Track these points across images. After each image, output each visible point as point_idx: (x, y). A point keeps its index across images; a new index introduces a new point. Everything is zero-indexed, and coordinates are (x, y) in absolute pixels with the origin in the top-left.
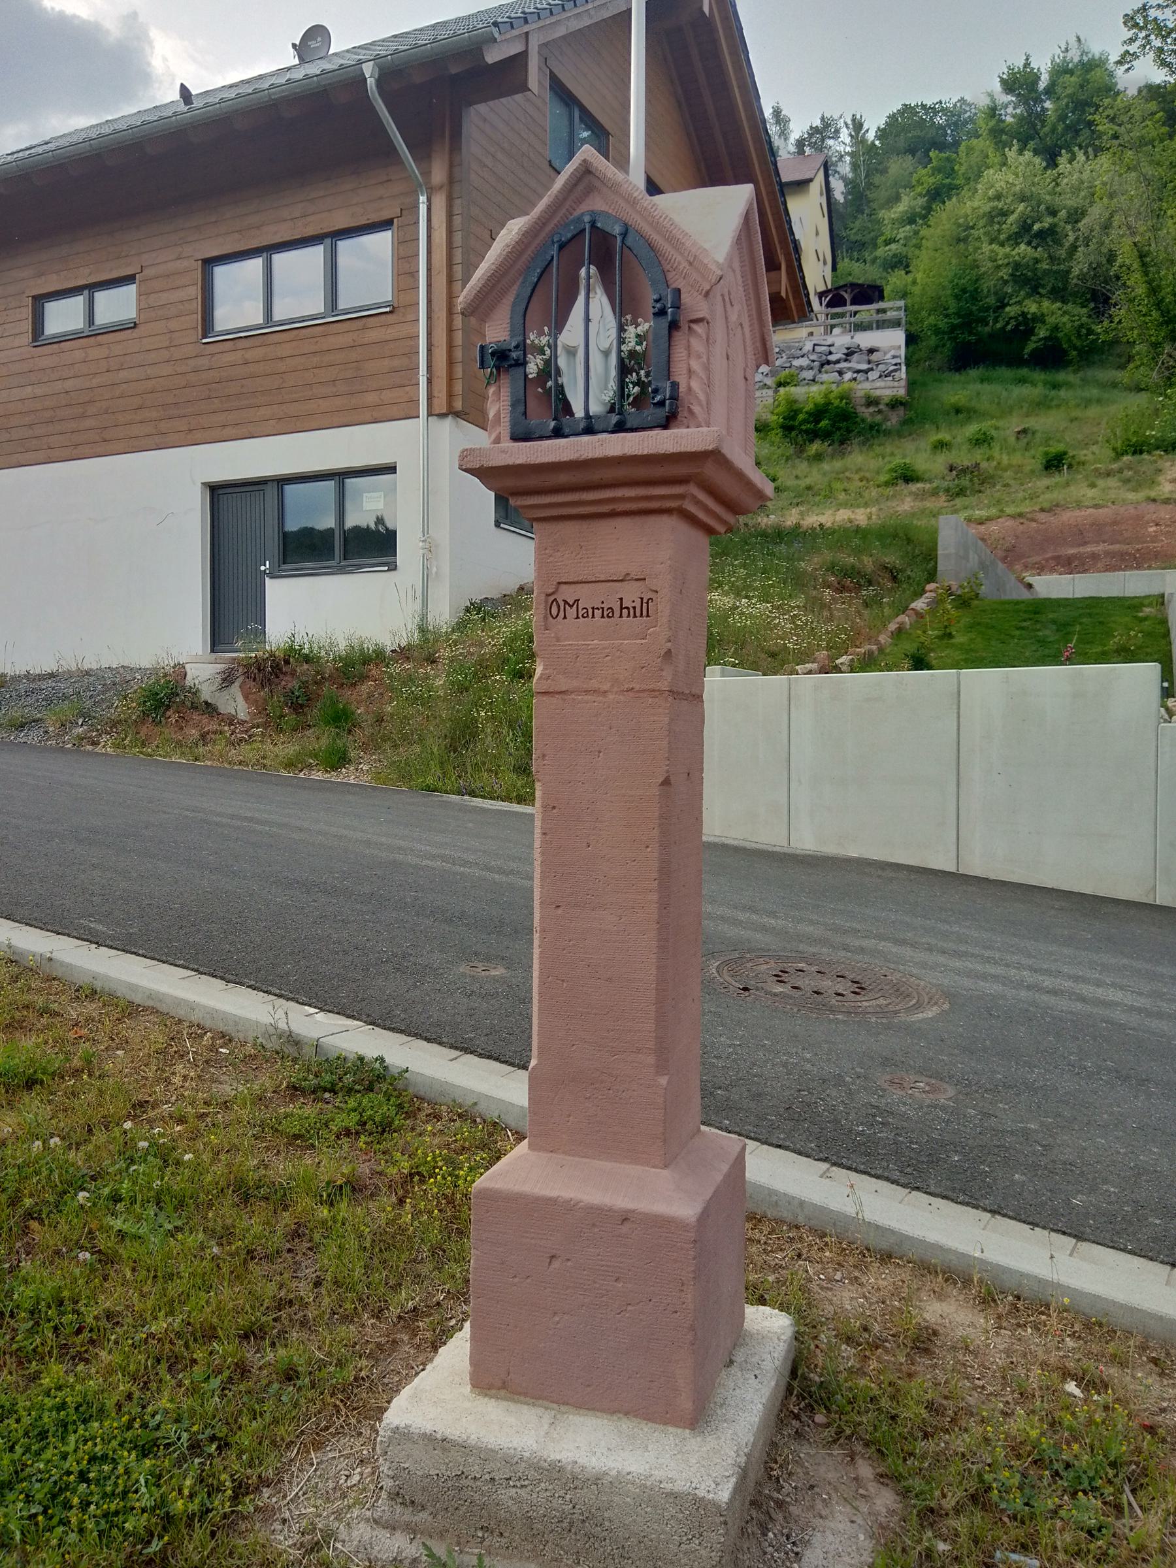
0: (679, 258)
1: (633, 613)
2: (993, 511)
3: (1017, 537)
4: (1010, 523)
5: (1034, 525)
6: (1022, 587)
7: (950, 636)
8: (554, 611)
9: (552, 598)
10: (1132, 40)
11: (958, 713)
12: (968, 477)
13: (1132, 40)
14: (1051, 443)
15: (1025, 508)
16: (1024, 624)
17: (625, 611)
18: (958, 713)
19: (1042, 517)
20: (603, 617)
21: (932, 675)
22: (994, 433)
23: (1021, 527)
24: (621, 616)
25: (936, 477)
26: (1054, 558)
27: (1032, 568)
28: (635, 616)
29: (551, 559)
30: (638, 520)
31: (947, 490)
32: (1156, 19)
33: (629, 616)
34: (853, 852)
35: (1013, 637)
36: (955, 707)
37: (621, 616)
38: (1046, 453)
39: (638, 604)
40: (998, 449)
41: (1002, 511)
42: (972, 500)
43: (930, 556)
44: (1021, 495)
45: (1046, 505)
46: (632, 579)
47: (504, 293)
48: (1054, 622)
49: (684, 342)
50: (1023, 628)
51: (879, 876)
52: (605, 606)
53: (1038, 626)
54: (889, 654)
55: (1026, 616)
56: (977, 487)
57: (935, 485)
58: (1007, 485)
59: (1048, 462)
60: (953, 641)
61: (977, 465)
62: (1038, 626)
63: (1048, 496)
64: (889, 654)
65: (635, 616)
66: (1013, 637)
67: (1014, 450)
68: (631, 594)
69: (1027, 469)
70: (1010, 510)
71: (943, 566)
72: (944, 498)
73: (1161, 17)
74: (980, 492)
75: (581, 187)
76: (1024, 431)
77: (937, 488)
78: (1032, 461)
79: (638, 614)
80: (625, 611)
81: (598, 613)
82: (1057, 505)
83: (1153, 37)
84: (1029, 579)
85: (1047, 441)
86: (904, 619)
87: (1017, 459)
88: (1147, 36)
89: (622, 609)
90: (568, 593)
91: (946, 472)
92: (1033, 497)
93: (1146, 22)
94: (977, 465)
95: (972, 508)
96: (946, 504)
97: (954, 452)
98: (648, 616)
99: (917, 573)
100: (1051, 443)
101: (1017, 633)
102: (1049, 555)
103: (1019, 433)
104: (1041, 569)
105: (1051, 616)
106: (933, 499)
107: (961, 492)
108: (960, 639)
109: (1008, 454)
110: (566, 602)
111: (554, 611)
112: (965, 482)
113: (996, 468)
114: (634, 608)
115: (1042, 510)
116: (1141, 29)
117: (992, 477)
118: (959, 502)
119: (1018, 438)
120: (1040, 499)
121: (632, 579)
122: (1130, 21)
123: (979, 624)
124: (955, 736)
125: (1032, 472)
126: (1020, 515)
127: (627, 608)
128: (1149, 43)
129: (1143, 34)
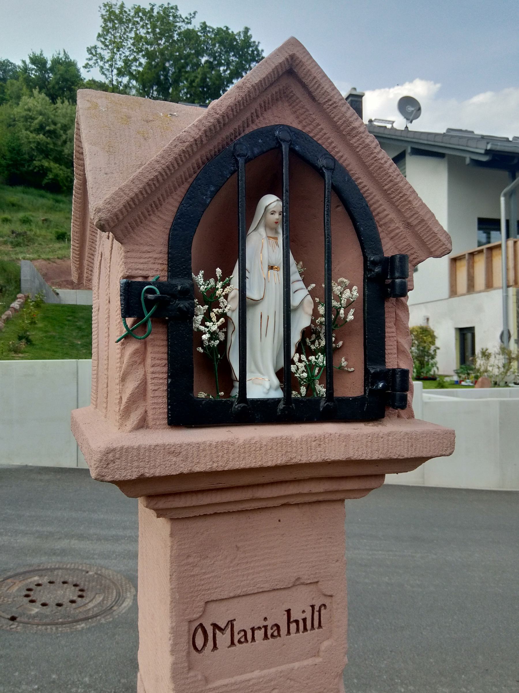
0: (392, 215)
1: (304, 626)
2: (35, 256)
3: (48, 269)
4: (44, 262)
5: (55, 264)
6: (54, 294)
7: (35, 323)
8: (200, 641)
9: (197, 624)
10: (90, 59)
11: (77, 383)
12: (22, 237)
13: (90, 59)
14: (58, 227)
15: (50, 256)
16: (69, 318)
17: (293, 626)
18: (77, 383)
19: (58, 261)
20: (266, 637)
21: (63, 362)
22: (32, 218)
23: (49, 265)
24: (289, 633)
25: (5, 236)
26: (65, 281)
27: (56, 285)
28: (305, 629)
29: (196, 570)
30: (306, 508)
31: (12, 243)
32: (100, 54)
33: (298, 630)
34: (17, 462)
35: (66, 325)
36: (76, 379)
37: (289, 633)
38: (57, 232)
39: (308, 615)
40: (34, 226)
41: (39, 256)
42: (24, 249)
43: (18, 282)
44: (48, 250)
45: (60, 256)
46: (303, 584)
47: (157, 206)
48: (83, 318)
49: (394, 315)
50: (69, 320)
51: (41, 480)
52: (269, 623)
53: (76, 320)
54: (4, 332)
55: (69, 314)
56: (26, 243)
57: (5, 239)
58: (40, 244)
59: (58, 236)
60: (37, 326)
61: (25, 232)
62: (76, 320)
63: (60, 252)
64: (4, 332)
65: (305, 629)
66: (66, 325)
67: (42, 228)
68: (300, 604)
69: (49, 238)
70: (43, 256)
71: (23, 285)
72: (10, 246)
73: (102, 54)
74: (28, 245)
75: (274, 90)
76: (46, 220)
77: (6, 241)
78: (51, 234)
79: (309, 626)
80: (293, 626)
81: (259, 634)
82: (65, 257)
83: (99, 61)
84: (58, 291)
85: (57, 226)
86: (9, 312)
87: (43, 232)
88: (96, 60)
89: (289, 622)
90: (220, 615)
91: (10, 233)
92: (53, 251)
93: (96, 54)
94: (25, 232)
95: (25, 253)
96: (11, 249)
97: (13, 224)
98: (320, 626)
99: (11, 288)
100: (58, 227)
101: (67, 323)
102: (63, 279)
103: (43, 220)
104: (60, 286)
105: (81, 315)
106: (5, 246)
107: (18, 245)
108: (40, 325)
109: (39, 229)
110: (215, 626)
111: (200, 641)
112: (20, 240)
113: (34, 235)
114: (304, 620)
115: (58, 258)
116: (94, 56)
117: (33, 239)
118: (18, 249)
119: (43, 223)
120: (57, 253)
121: (303, 584)
122: (89, 50)
123: (48, 317)
124: (76, 394)
125: (51, 239)
126: (48, 259)
127: (297, 622)
128: (97, 62)
129: (95, 58)
